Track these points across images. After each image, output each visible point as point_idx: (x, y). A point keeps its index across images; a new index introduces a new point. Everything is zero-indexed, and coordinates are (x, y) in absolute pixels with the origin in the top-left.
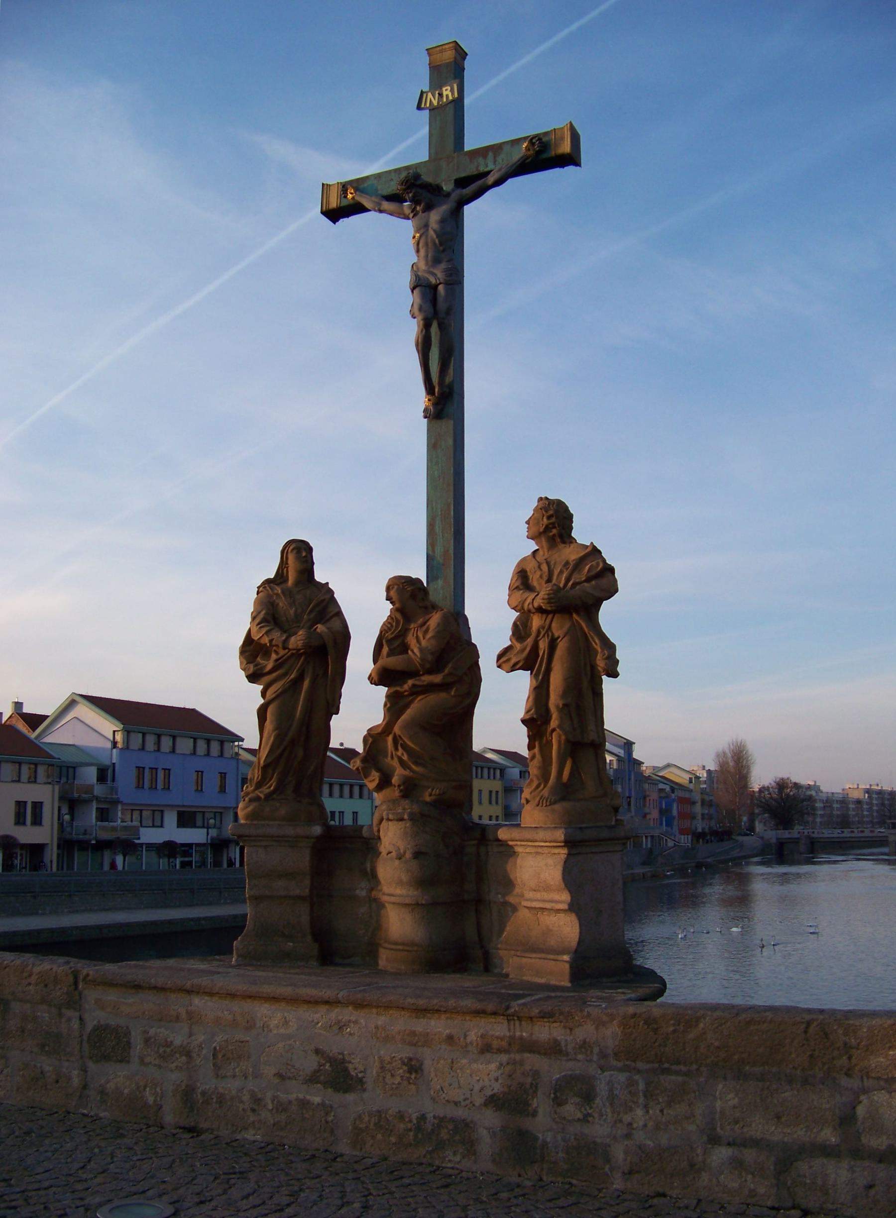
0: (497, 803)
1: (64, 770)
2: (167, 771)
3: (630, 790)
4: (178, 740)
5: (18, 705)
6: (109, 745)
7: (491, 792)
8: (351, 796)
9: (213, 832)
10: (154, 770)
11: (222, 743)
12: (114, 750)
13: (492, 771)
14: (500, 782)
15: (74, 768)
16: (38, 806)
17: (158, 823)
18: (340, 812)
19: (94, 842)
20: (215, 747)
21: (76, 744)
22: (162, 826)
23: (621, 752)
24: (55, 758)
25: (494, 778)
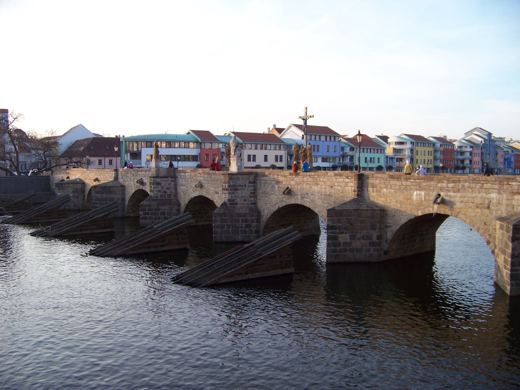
0: (431, 155)
1: (288, 146)
2: (318, 146)
3: (490, 152)
4: (321, 137)
5: (275, 125)
6: (301, 139)
7: (429, 151)
8: (377, 153)
9: (333, 164)
11: (335, 137)
13: (424, 144)
14: (432, 148)
16: (281, 156)
17: (316, 161)
21: (292, 138)
22: (317, 162)
23: (486, 137)
24: (285, 143)
25: (430, 147)
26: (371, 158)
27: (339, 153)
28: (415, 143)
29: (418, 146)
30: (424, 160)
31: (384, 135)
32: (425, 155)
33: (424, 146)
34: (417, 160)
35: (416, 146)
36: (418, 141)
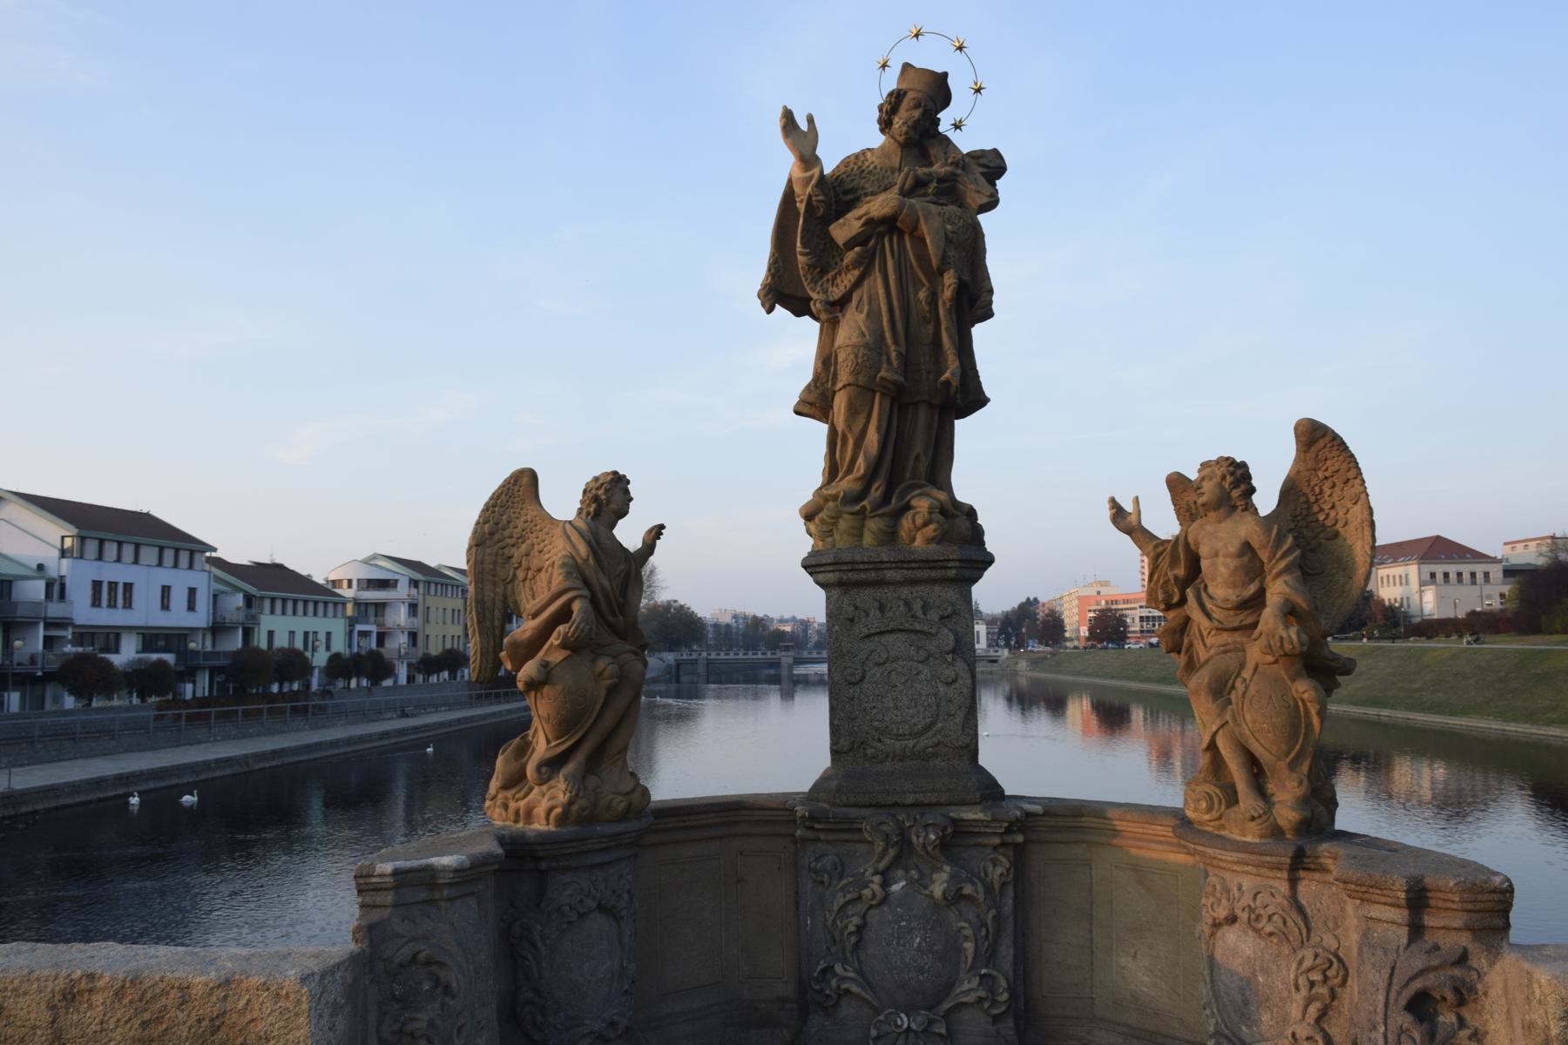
2: (128, 587)
6: (56, 553)
7: (453, 610)
10: (113, 586)
11: (192, 553)
12: (64, 561)
15: (11, 582)
18: (314, 632)
19: (40, 674)
20: (184, 558)
26: (306, 634)
27: (200, 618)
28: (421, 586)
29: (429, 593)
30: (444, 636)
31: (278, 561)
32: (444, 623)
33: (444, 594)
34: (428, 636)
35: (424, 595)
36: (430, 578)
